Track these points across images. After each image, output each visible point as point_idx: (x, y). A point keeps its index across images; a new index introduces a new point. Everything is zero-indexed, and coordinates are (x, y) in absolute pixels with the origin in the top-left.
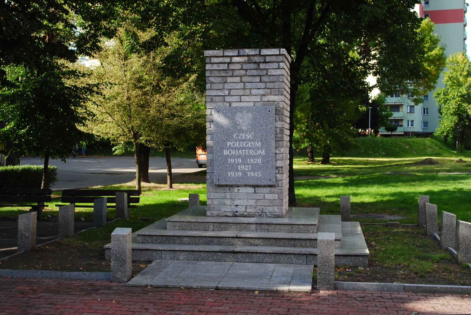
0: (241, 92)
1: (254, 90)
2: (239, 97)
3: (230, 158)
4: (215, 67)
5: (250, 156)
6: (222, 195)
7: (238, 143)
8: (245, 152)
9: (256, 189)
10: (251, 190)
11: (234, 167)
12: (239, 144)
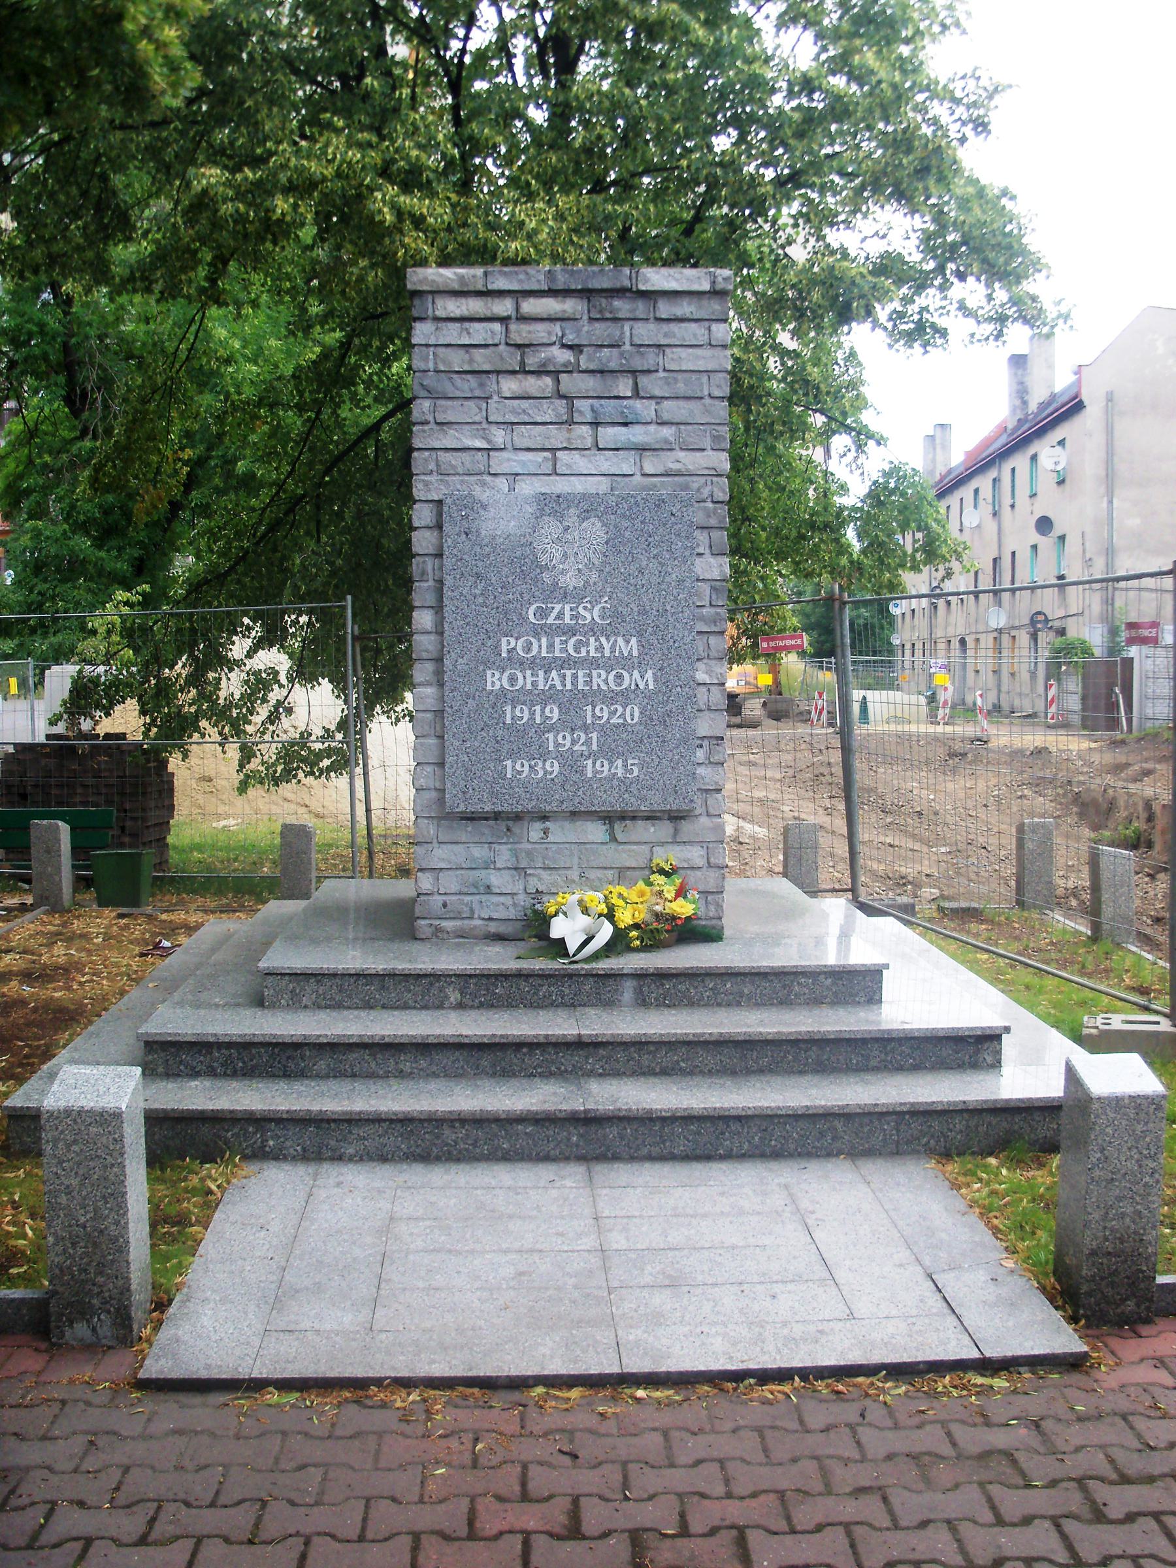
0: (557, 437)
1: (611, 431)
2: (547, 454)
3: (514, 703)
4: (452, 334)
5: (594, 697)
6: (479, 852)
7: (544, 640)
8: (575, 677)
9: (618, 826)
10: (595, 832)
11: (527, 741)
12: (551, 646)
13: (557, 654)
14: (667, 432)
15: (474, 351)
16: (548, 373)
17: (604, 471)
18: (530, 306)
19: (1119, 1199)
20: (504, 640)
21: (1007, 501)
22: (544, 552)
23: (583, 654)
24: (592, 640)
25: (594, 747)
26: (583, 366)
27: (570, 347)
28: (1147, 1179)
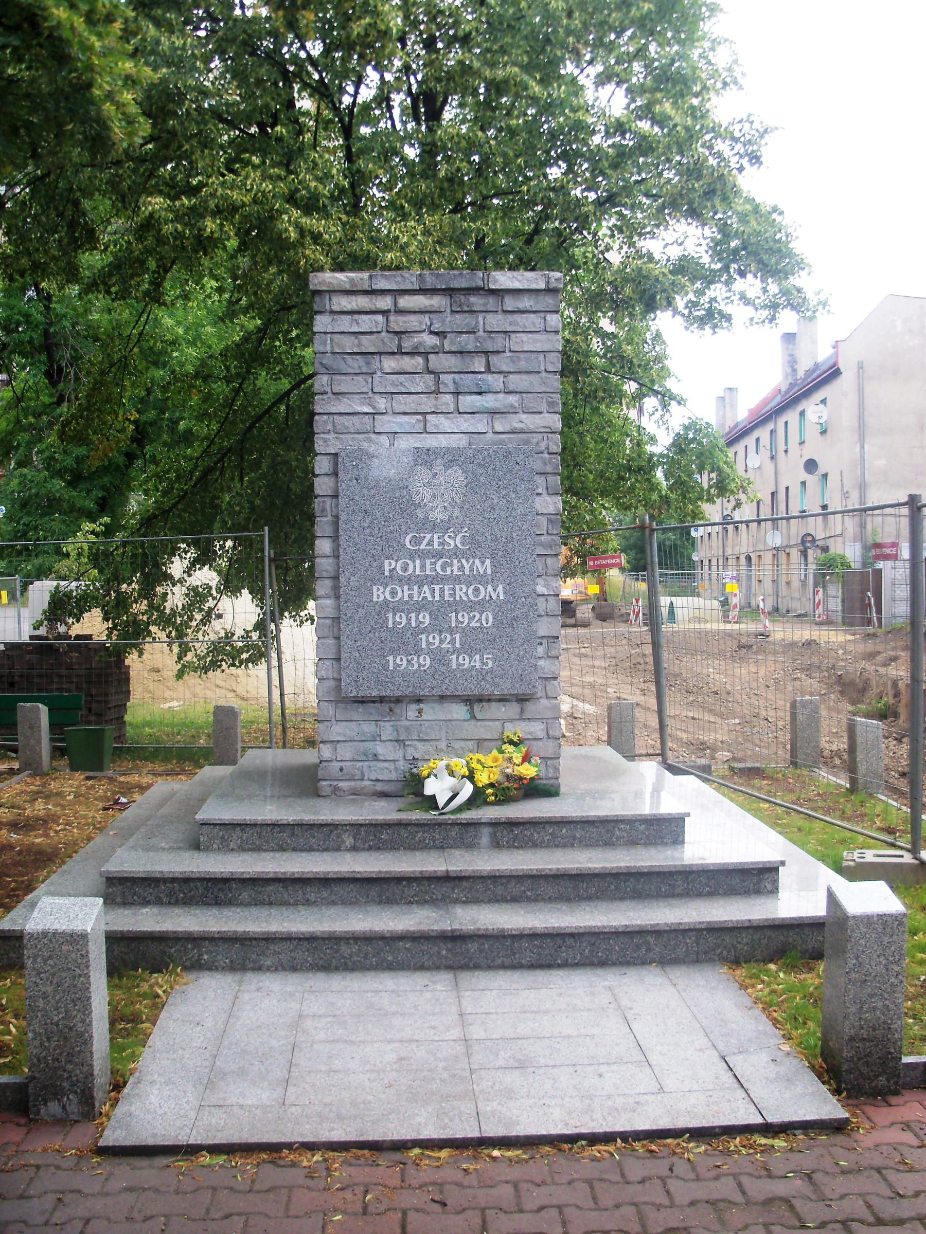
0: (427, 404)
4: (345, 324)
5: (456, 606)
6: (368, 728)
7: (418, 562)
8: (442, 591)
10: (459, 711)
11: (406, 641)
12: (423, 567)
13: (428, 572)
14: (513, 399)
15: (361, 337)
16: (419, 354)
17: (463, 429)
18: (405, 302)
19: (871, 996)
20: (386, 562)
21: (781, 447)
22: (418, 493)
23: (449, 572)
24: (455, 561)
25: (458, 645)
26: (447, 348)
27: (437, 334)
28: (893, 980)
